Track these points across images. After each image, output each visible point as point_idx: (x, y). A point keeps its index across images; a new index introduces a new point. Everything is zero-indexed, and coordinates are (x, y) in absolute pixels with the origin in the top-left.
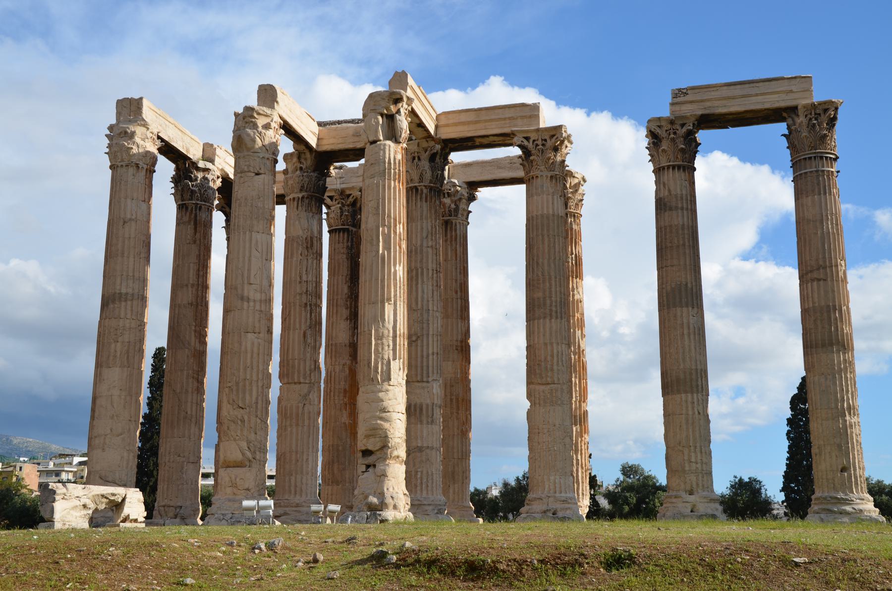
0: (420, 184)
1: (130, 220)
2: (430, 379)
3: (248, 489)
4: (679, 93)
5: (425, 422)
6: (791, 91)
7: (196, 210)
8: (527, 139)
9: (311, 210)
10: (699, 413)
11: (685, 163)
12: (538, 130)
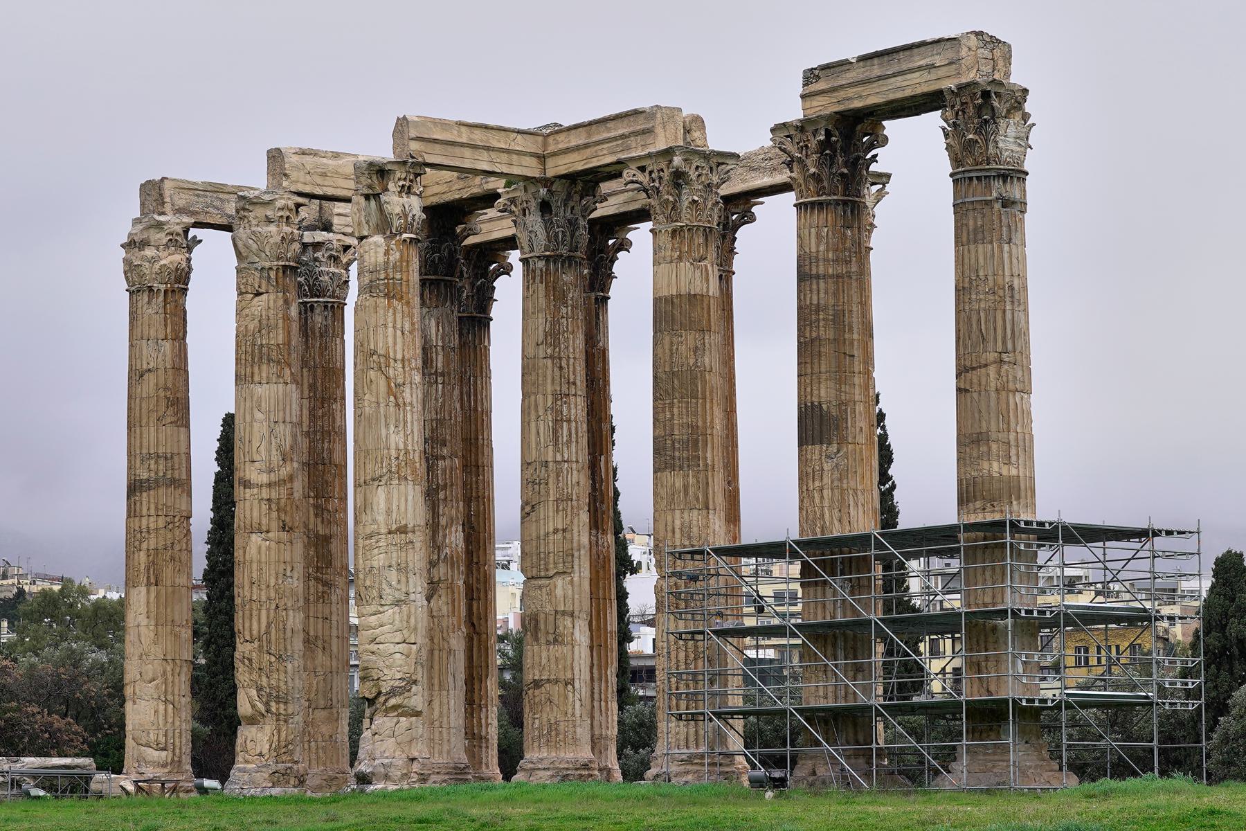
4: (811, 76)
11: (823, 198)
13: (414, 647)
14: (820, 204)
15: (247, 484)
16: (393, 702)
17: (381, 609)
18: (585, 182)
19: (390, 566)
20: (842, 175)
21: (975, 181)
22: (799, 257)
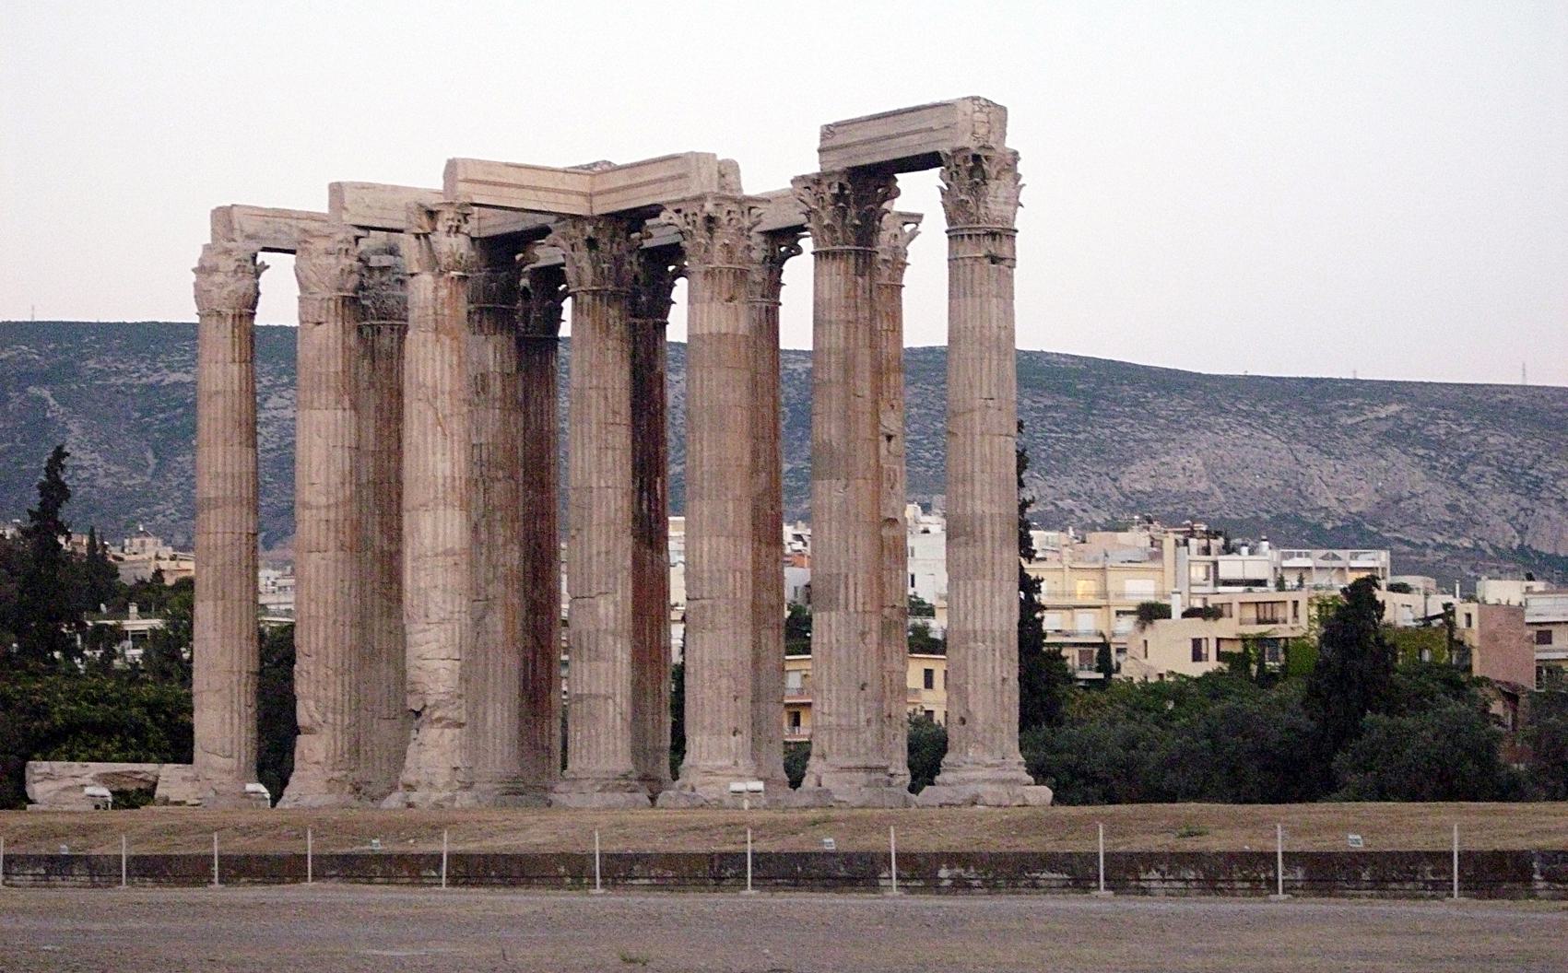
0: (579, 289)
1: (217, 393)
2: (594, 593)
3: (317, 763)
4: (829, 131)
5: (585, 658)
6: (931, 129)
7: (373, 335)
8: (678, 211)
9: (483, 331)
10: (838, 641)
11: (837, 247)
12: (683, 200)
13: (457, 663)
14: (834, 254)
15: (306, 506)
16: (437, 714)
17: (427, 627)
18: (633, 220)
19: (436, 587)
20: (856, 226)
21: (966, 238)
22: (816, 304)
